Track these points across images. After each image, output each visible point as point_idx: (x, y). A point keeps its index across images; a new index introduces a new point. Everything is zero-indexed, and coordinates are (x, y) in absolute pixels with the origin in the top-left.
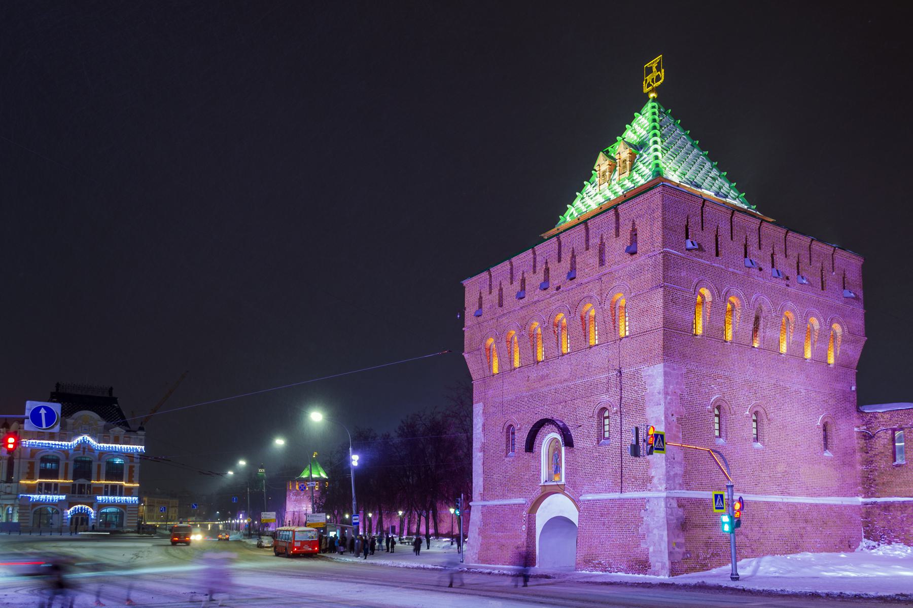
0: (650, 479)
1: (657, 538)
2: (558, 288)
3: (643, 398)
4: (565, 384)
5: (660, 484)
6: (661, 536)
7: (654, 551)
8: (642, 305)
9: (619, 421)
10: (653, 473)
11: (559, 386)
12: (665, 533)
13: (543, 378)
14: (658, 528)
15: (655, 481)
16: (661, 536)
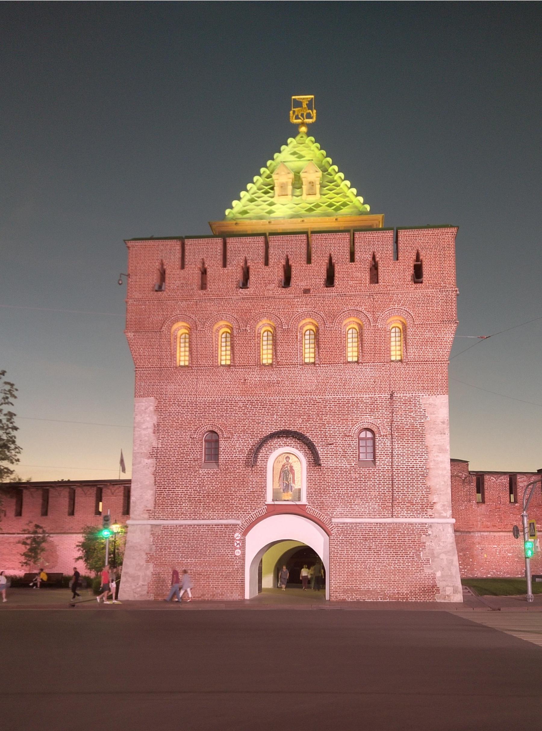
0: (432, 506)
1: (445, 562)
2: (307, 291)
3: (422, 425)
4: (308, 397)
5: (445, 510)
6: (451, 562)
7: (442, 576)
8: (428, 335)
9: (389, 444)
10: (435, 498)
11: (298, 397)
12: (456, 558)
13: (270, 384)
14: (446, 553)
15: (438, 507)
16: (451, 562)
